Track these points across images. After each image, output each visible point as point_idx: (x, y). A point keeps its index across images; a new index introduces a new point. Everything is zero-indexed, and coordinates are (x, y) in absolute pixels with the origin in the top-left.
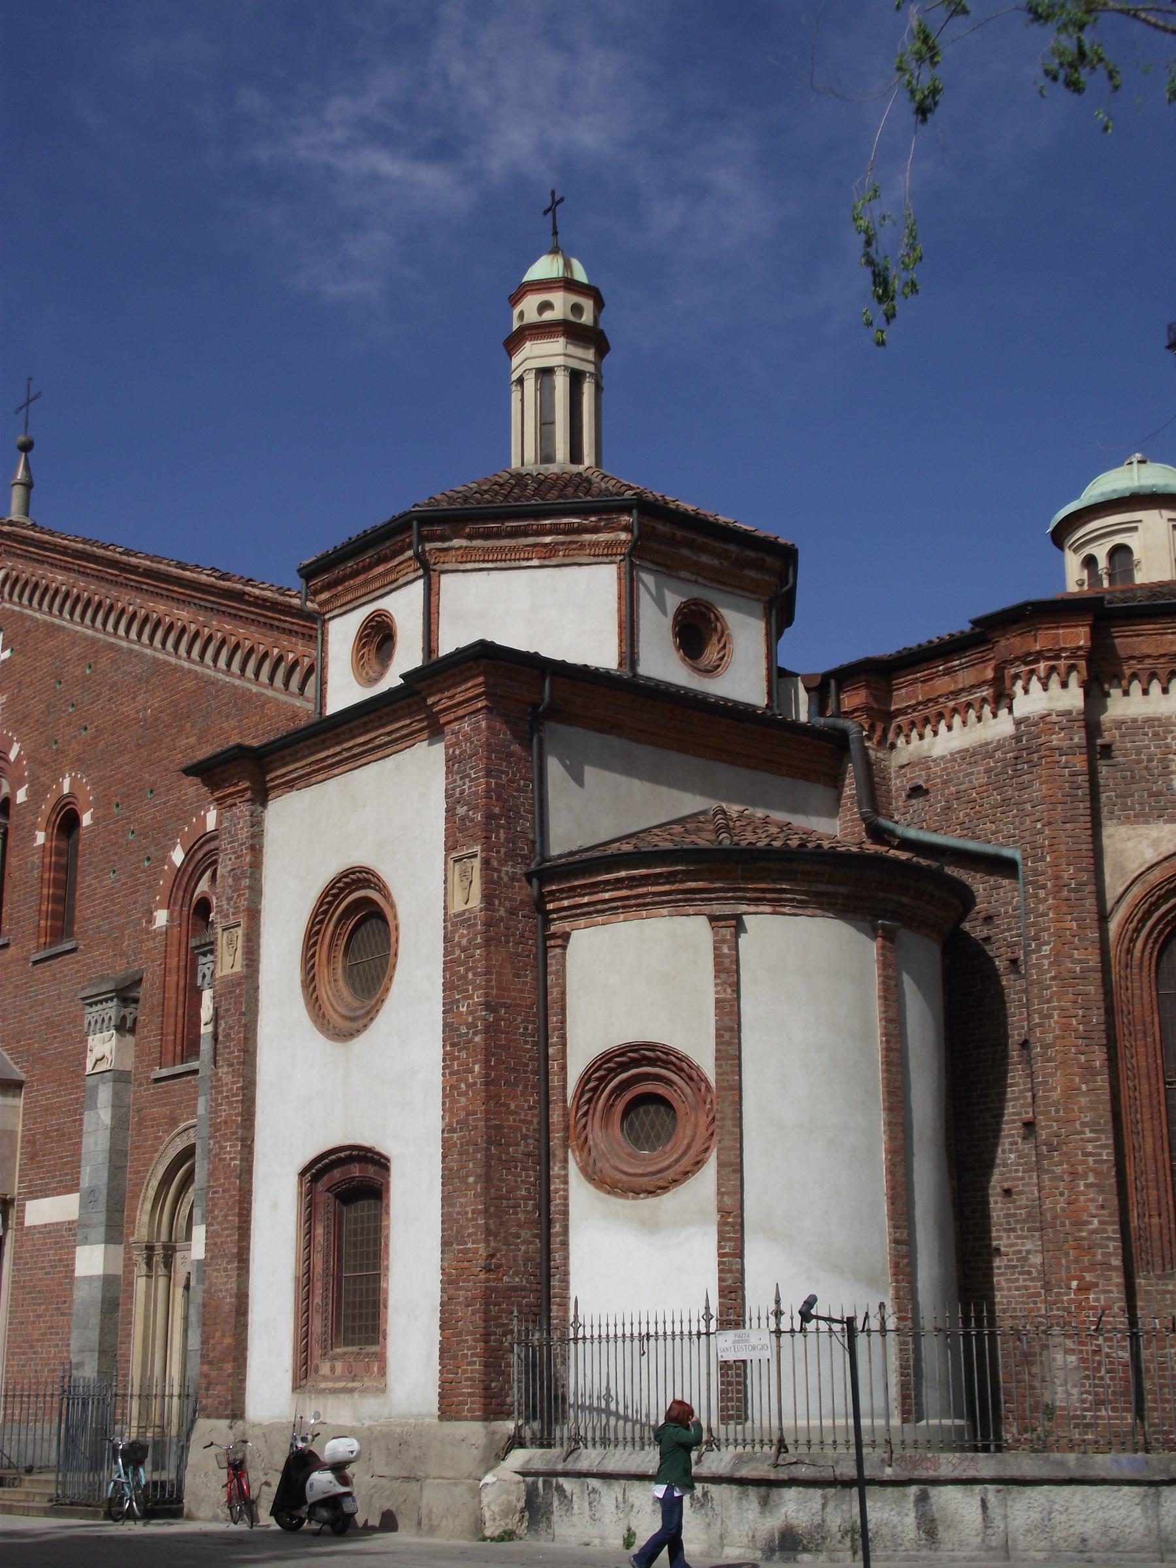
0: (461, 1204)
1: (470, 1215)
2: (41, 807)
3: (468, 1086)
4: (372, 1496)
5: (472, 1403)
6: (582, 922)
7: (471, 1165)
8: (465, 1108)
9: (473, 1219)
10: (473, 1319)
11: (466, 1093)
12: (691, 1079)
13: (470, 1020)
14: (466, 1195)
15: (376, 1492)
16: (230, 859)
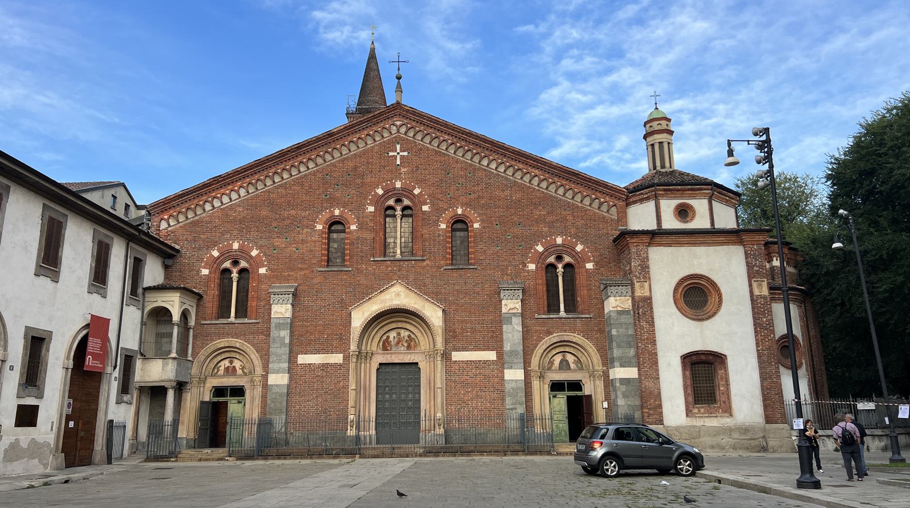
2: (442, 215)
3: (769, 340)
11: (768, 342)
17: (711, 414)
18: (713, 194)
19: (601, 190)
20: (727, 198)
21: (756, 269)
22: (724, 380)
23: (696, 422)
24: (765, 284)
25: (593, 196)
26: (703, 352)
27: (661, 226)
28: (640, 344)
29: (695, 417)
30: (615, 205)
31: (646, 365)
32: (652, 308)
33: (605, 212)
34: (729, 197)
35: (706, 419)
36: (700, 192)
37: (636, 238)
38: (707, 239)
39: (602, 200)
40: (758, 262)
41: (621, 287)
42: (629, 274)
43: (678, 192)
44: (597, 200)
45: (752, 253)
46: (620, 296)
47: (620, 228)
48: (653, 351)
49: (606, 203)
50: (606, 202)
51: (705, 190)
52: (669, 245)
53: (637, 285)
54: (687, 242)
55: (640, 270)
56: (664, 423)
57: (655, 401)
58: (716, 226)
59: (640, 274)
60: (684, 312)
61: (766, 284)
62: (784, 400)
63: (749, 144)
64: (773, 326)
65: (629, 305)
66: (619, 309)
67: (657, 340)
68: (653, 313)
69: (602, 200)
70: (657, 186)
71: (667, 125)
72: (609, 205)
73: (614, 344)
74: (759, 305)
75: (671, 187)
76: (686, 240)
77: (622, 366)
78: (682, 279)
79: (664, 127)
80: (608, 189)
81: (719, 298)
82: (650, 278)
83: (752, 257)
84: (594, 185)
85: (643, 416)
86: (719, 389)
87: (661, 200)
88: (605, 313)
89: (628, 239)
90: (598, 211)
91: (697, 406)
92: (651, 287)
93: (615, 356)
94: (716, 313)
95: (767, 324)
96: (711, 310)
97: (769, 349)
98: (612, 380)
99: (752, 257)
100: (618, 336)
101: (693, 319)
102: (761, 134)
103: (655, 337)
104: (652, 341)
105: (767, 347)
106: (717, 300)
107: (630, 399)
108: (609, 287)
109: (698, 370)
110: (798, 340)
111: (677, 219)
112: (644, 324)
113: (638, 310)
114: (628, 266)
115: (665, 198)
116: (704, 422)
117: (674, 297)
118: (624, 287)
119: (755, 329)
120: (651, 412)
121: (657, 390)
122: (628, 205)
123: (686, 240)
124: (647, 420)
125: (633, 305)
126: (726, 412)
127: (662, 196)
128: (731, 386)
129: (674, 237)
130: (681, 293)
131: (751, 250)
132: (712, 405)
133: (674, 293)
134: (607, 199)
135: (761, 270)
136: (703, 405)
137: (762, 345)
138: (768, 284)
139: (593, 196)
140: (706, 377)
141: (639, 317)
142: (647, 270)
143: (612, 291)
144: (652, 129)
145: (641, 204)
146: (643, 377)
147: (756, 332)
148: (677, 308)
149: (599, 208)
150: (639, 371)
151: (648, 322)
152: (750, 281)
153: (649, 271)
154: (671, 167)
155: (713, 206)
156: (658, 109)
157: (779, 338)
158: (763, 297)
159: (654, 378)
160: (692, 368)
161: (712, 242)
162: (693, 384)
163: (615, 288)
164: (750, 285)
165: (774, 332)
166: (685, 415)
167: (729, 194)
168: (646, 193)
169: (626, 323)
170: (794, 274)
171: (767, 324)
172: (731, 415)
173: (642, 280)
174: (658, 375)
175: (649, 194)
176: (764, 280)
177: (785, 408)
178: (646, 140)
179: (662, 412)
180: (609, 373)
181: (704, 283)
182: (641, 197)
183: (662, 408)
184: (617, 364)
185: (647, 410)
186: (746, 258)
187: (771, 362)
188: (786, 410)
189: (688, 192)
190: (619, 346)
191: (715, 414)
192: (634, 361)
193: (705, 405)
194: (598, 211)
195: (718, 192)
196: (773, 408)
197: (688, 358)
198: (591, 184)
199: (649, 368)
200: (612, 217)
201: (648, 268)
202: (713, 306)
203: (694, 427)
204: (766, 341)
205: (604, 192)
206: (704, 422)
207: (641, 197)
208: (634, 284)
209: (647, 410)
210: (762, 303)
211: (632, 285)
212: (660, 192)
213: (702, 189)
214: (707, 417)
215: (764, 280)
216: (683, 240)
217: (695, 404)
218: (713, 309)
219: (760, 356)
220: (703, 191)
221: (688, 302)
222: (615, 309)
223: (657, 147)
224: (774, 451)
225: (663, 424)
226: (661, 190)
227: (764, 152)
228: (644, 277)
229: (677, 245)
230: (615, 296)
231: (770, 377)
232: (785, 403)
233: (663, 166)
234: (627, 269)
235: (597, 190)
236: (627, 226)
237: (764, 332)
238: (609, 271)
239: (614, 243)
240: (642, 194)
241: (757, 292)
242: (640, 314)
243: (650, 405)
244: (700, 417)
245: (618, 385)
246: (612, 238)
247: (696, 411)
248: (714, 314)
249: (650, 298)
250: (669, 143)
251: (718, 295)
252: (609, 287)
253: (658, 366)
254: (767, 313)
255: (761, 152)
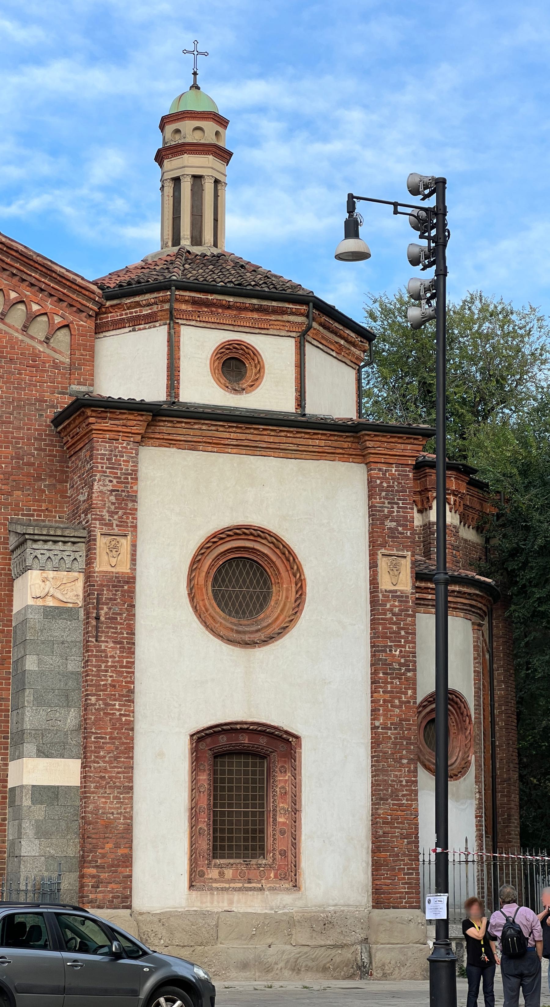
0: (396, 776)
1: (404, 783)
4: (298, 958)
5: (409, 898)
6: (422, 609)
7: (404, 752)
8: (397, 716)
9: (406, 786)
10: (409, 846)
11: (400, 707)
12: (462, 714)
13: (402, 661)
14: (400, 771)
15: (300, 957)
16: (111, 481)
17: (250, 883)
18: (309, 328)
19: (33, 281)
20: (342, 342)
21: (390, 524)
22: (289, 800)
23: (212, 903)
24: (406, 566)
25: (13, 295)
26: (245, 726)
27: (177, 396)
28: (93, 699)
29: (211, 889)
30: (67, 326)
31: (102, 754)
32: (134, 606)
33: (41, 342)
34: (346, 340)
35: (236, 896)
36: (279, 318)
37: (110, 419)
38: (284, 440)
39: (35, 307)
40: (395, 509)
41: (60, 546)
42: (86, 512)
43: (228, 312)
44: (21, 307)
45: (385, 485)
46: (56, 569)
47: (75, 387)
48: (124, 719)
49: (44, 318)
50: (46, 314)
51: (292, 313)
52: (193, 446)
53: (101, 542)
54: (235, 443)
55: (113, 504)
56: (134, 905)
57: (117, 846)
58: (309, 410)
59: (112, 514)
60: (210, 621)
61: (409, 565)
62: (421, 850)
63: (396, 212)
64: (414, 670)
65: (77, 595)
66: (50, 603)
67: (136, 690)
68: (134, 620)
69: (35, 307)
70: (178, 288)
71: (217, 133)
72: (50, 322)
73: (28, 696)
74: (389, 615)
75: (210, 297)
76: (233, 436)
77: (42, 753)
78: (214, 536)
79: (209, 138)
80: (53, 279)
81: (297, 593)
82: (135, 527)
83: (384, 494)
84: (18, 265)
85: (82, 886)
86: (275, 820)
87: (182, 327)
88: (14, 612)
89: (91, 420)
90: (20, 337)
91: (218, 861)
92: (135, 551)
93: (27, 726)
94: (284, 628)
95: (400, 664)
96: (277, 619)
97: (398, 725)
98: (13, 789)
99: (384, 494)
100: (42, 673)
101: (230, 641)
102: (427, 192)
103: (133, 683)
104: (124, 692)
105: (396, 720)
106: (293, 596)
107: (54, 841)
108: (29, 543)
109: (230, 772)
110: (465, 703)
111: (218, 381)
112: (108, 646)
113: (98, 609)
114: (86, 490)
115: (193, 323)
116: (231, 902)
117: (190, 580)
118: (69, 547)
119: (374, 674)
120: (104, 876)
121: (125, 818)
122: (100, 329)
123: (233, 436)
124: (91, 896)
125: (87, 595)
126: (285, 878)
127: (188, 317)
128: (303, 815)
129: (204, 427)
130: (208, 573)
131: (384, 478)
132: (254, 861)
133: (192, 570)
134: (49, 305)
135: (400, 529)
136: (232, 861)
137: (385, 715)
138: (414, 563)
139: (13, 295)
140: (246, 789)
141: (97, 627)
142: (130, 505)
143: (37, 552)
144: (178, 139)
145: (134, 330)
146: (93, 785)
147: (374, 682)
148: (195, 608)
149: (25, 328)
150: (84, 767)
151: (121, 643)
152: (373, 556)
153: (136, 510)
154: (215, 245)
155: (307, 357)
156: (198, 88)
157: (426, 700)
158: (398, 597)
159: (119, 788)
160: (215, 764)
161: (295, 448)
162: (215, 805)
163: (46, 547)
164: (373, 565)
165: (415, 684)
166: (186, 884)
167: (348, 332)
168: (149, 305)
169: (63, 643)
170: (474, 545)
171: (400, 664)
172: (296, 886)
173: (116, 530)
174: (131, 779)
175: (155, 308)
176: (405, 553)
177: (421, 871)
178: (161, 164)
179: (131, 876)
180: (7, 770)
181: (266, 551)
182: (136, 312)
183: (131, 866)
184: (29, 747)
185: (93, 871)
186: (370, 497)
187: (401, 758)
188: (421, 876)
189: (250, 315)
190: (39, 701)
191: (259, 882)
192: (76, 740)
193: (238, 861)
194: (20, 337)
195: (321, 324)
196: (394, 870)
197: (209, 740)
198: (8, 261)
199: (110, 762)
200: (57, 356)
201: (134, 499)
202: (282, 610)
203: (205, 914)
204: (395, 707)
205: (43, 286)
206: (231, 902)
207: (136, 312)
208: (95, 540)
209: (93, 871)
210: (396, 610)
211: (90, 541)
212: (184, 307)
213: (283, 312)
214: (240, 889)
215: (405, 553)
216: (227, 435)
217: (214, 857)
218: (282, 618)
219: (376, 743)
220: (286, 318)
221: (223, 596)
222: (40, 602)
223: (186, 186)
224: (385, 976)
225: (129, 907)
226: (186, 302)
227: (429, 238)
228: (122, 524)
229: (210, 449)
230: (42, 569)
231: (394, 795)
232: (421, 858)
233: (197, 240)
234: (82, 498)
235: (23, 280)
236: (92, 385)
237: (392, 683)
238: (35, 500)
239: (56, 427)
240: (138, 304)
241: (385, 584)
242: (102, 619)
243: (103, 856)
244: (222, 889)
245: (27, 802)
246: (50, 413)
247: (214, 873)
248: (283, 630)
249: (134, 578)
250: (217, 182)
251: (296, 585)
252: (29, 543)
253: (132, 758)
254: (402, 637)
255: (421, 237)
